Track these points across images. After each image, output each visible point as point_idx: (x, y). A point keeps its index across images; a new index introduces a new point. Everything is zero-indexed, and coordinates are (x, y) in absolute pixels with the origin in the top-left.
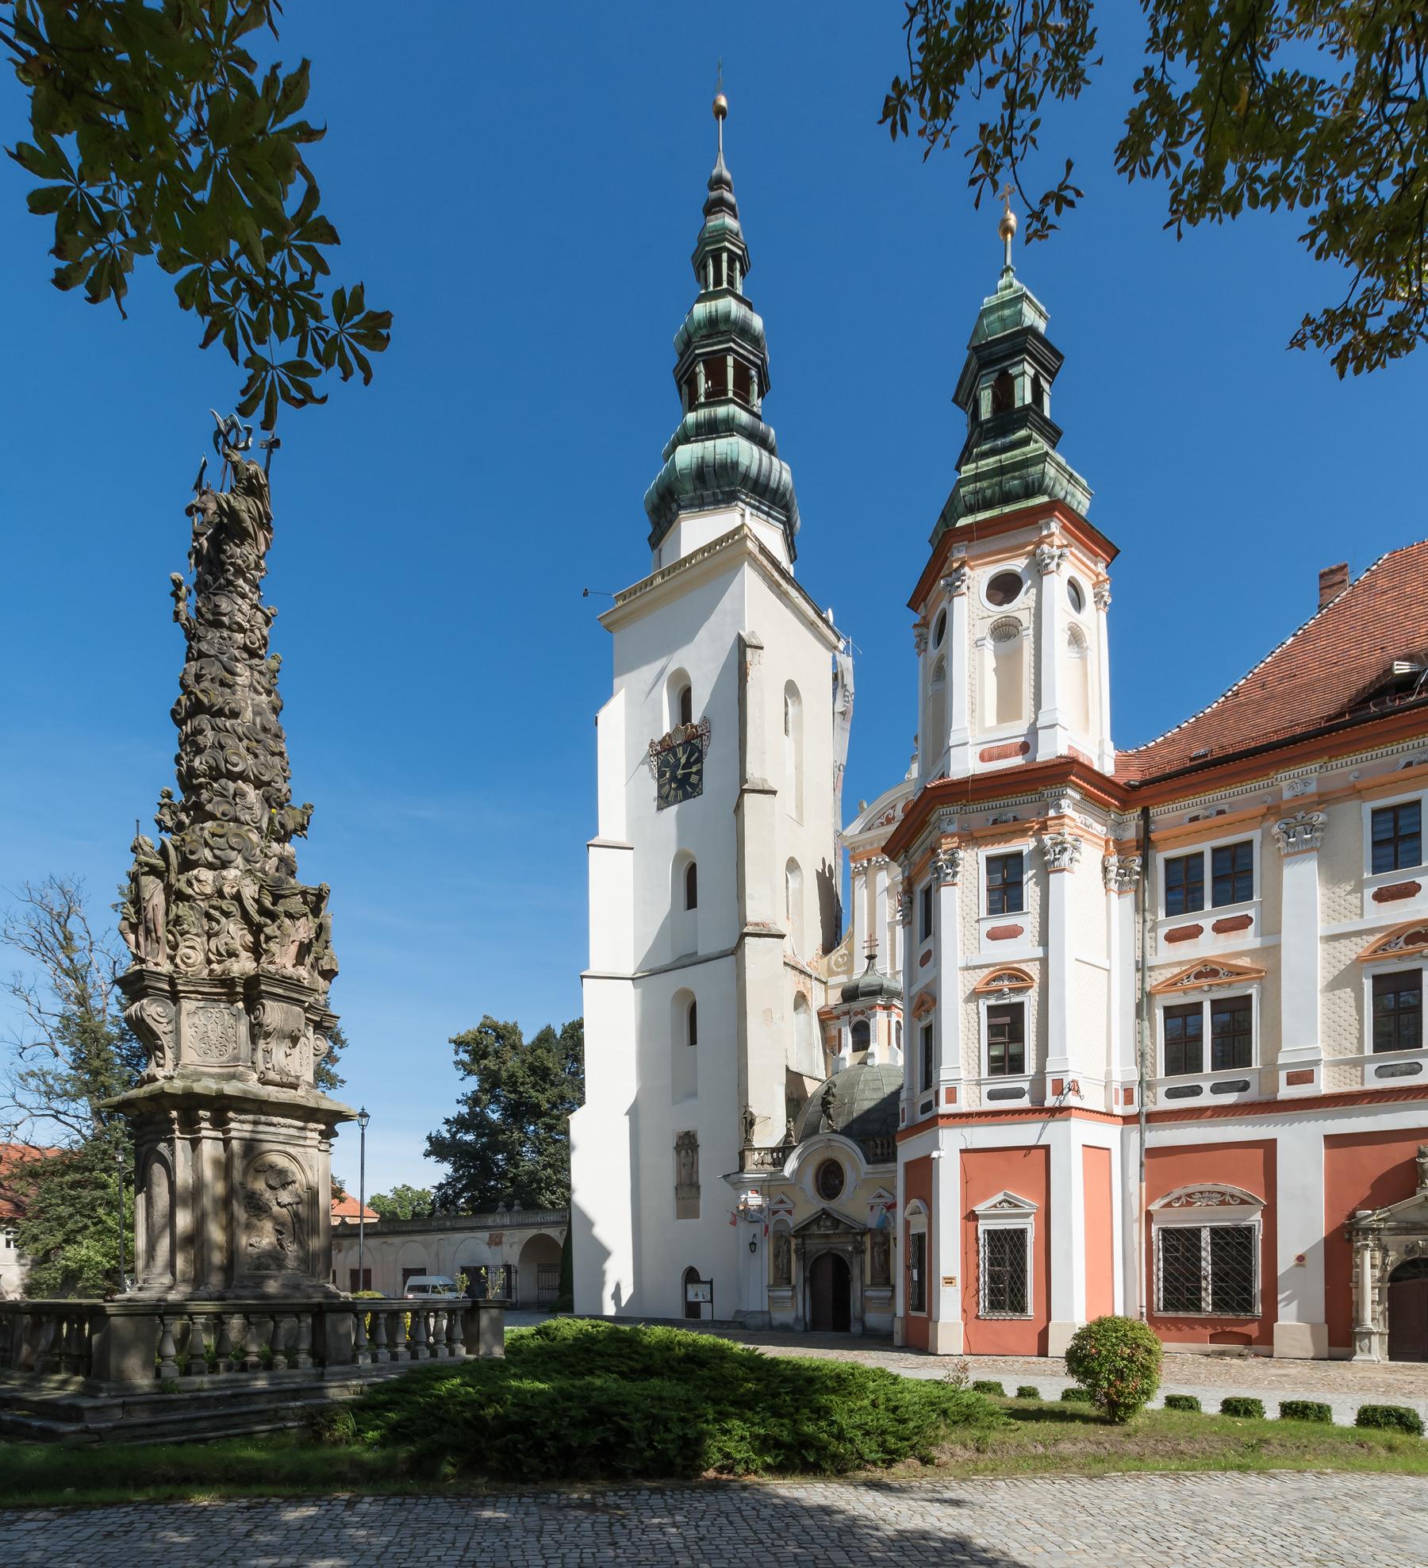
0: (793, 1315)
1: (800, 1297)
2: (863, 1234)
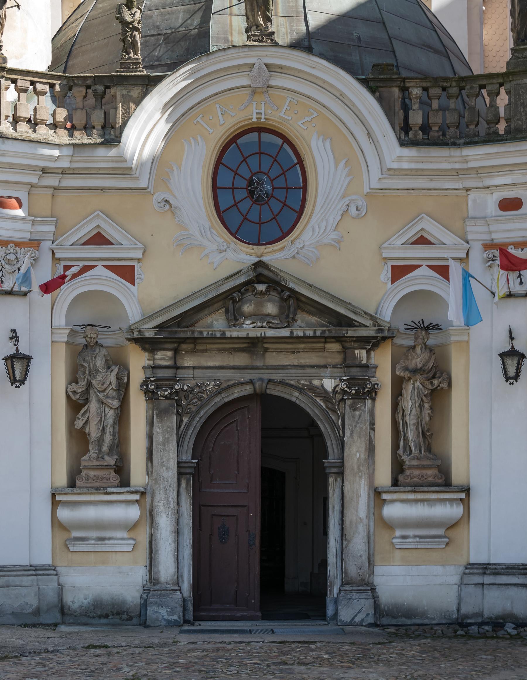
0: (139, 575)
1: (165, 522)
2: (372, 343)
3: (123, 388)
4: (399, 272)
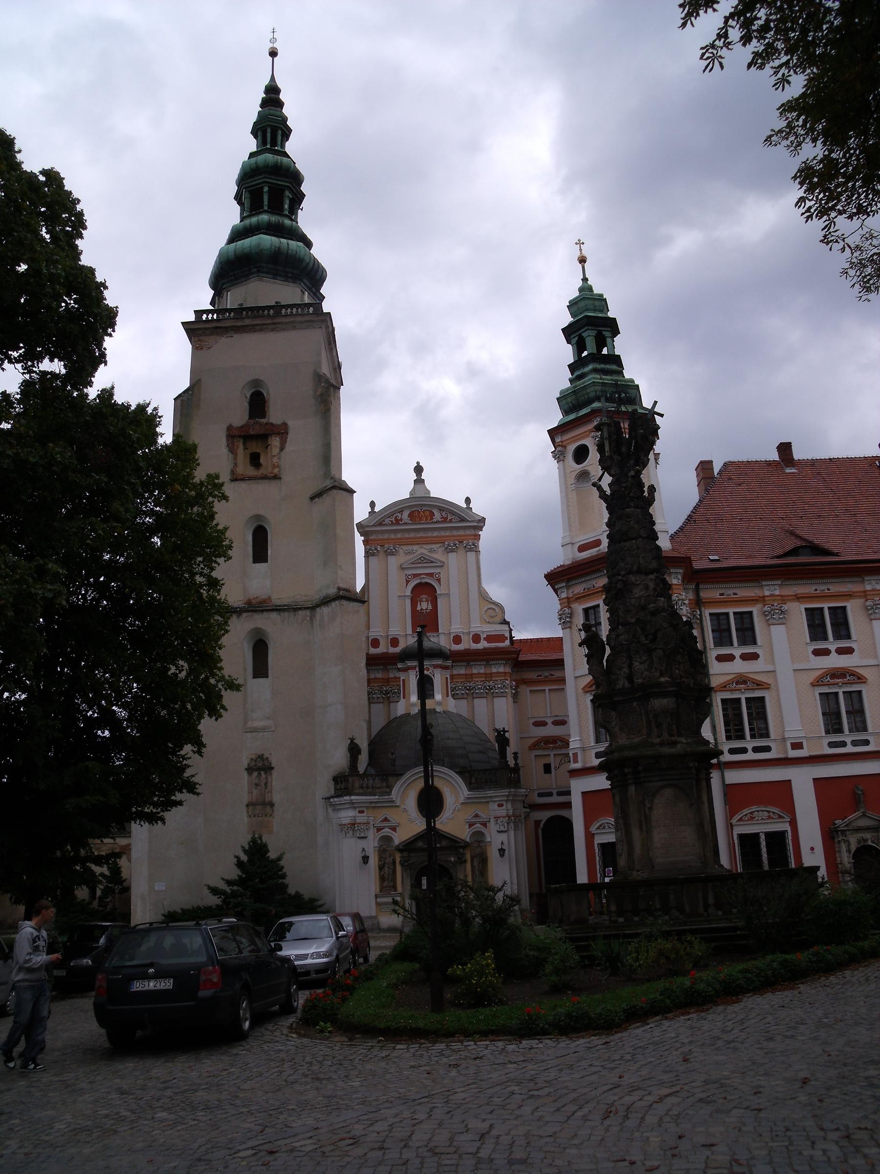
3: (394, 862)
4: (471, 825)
